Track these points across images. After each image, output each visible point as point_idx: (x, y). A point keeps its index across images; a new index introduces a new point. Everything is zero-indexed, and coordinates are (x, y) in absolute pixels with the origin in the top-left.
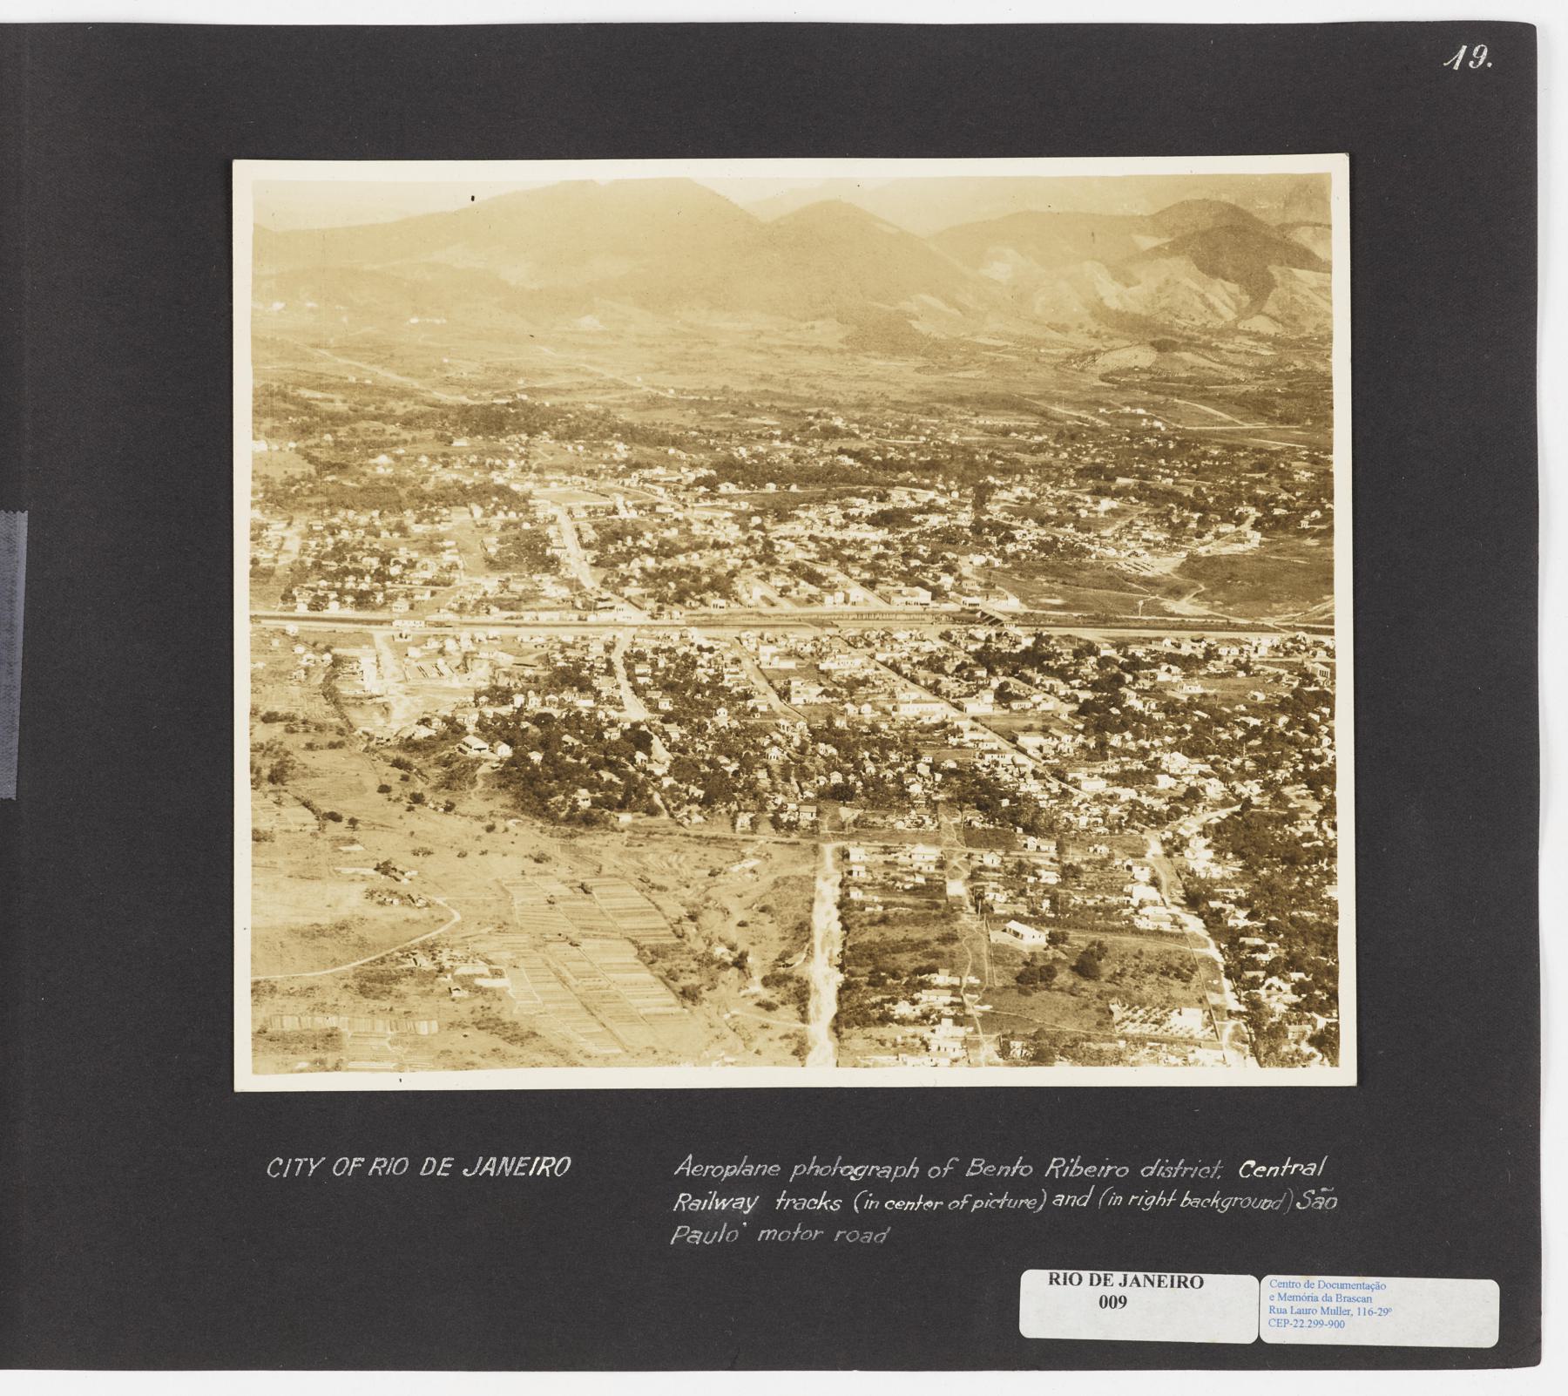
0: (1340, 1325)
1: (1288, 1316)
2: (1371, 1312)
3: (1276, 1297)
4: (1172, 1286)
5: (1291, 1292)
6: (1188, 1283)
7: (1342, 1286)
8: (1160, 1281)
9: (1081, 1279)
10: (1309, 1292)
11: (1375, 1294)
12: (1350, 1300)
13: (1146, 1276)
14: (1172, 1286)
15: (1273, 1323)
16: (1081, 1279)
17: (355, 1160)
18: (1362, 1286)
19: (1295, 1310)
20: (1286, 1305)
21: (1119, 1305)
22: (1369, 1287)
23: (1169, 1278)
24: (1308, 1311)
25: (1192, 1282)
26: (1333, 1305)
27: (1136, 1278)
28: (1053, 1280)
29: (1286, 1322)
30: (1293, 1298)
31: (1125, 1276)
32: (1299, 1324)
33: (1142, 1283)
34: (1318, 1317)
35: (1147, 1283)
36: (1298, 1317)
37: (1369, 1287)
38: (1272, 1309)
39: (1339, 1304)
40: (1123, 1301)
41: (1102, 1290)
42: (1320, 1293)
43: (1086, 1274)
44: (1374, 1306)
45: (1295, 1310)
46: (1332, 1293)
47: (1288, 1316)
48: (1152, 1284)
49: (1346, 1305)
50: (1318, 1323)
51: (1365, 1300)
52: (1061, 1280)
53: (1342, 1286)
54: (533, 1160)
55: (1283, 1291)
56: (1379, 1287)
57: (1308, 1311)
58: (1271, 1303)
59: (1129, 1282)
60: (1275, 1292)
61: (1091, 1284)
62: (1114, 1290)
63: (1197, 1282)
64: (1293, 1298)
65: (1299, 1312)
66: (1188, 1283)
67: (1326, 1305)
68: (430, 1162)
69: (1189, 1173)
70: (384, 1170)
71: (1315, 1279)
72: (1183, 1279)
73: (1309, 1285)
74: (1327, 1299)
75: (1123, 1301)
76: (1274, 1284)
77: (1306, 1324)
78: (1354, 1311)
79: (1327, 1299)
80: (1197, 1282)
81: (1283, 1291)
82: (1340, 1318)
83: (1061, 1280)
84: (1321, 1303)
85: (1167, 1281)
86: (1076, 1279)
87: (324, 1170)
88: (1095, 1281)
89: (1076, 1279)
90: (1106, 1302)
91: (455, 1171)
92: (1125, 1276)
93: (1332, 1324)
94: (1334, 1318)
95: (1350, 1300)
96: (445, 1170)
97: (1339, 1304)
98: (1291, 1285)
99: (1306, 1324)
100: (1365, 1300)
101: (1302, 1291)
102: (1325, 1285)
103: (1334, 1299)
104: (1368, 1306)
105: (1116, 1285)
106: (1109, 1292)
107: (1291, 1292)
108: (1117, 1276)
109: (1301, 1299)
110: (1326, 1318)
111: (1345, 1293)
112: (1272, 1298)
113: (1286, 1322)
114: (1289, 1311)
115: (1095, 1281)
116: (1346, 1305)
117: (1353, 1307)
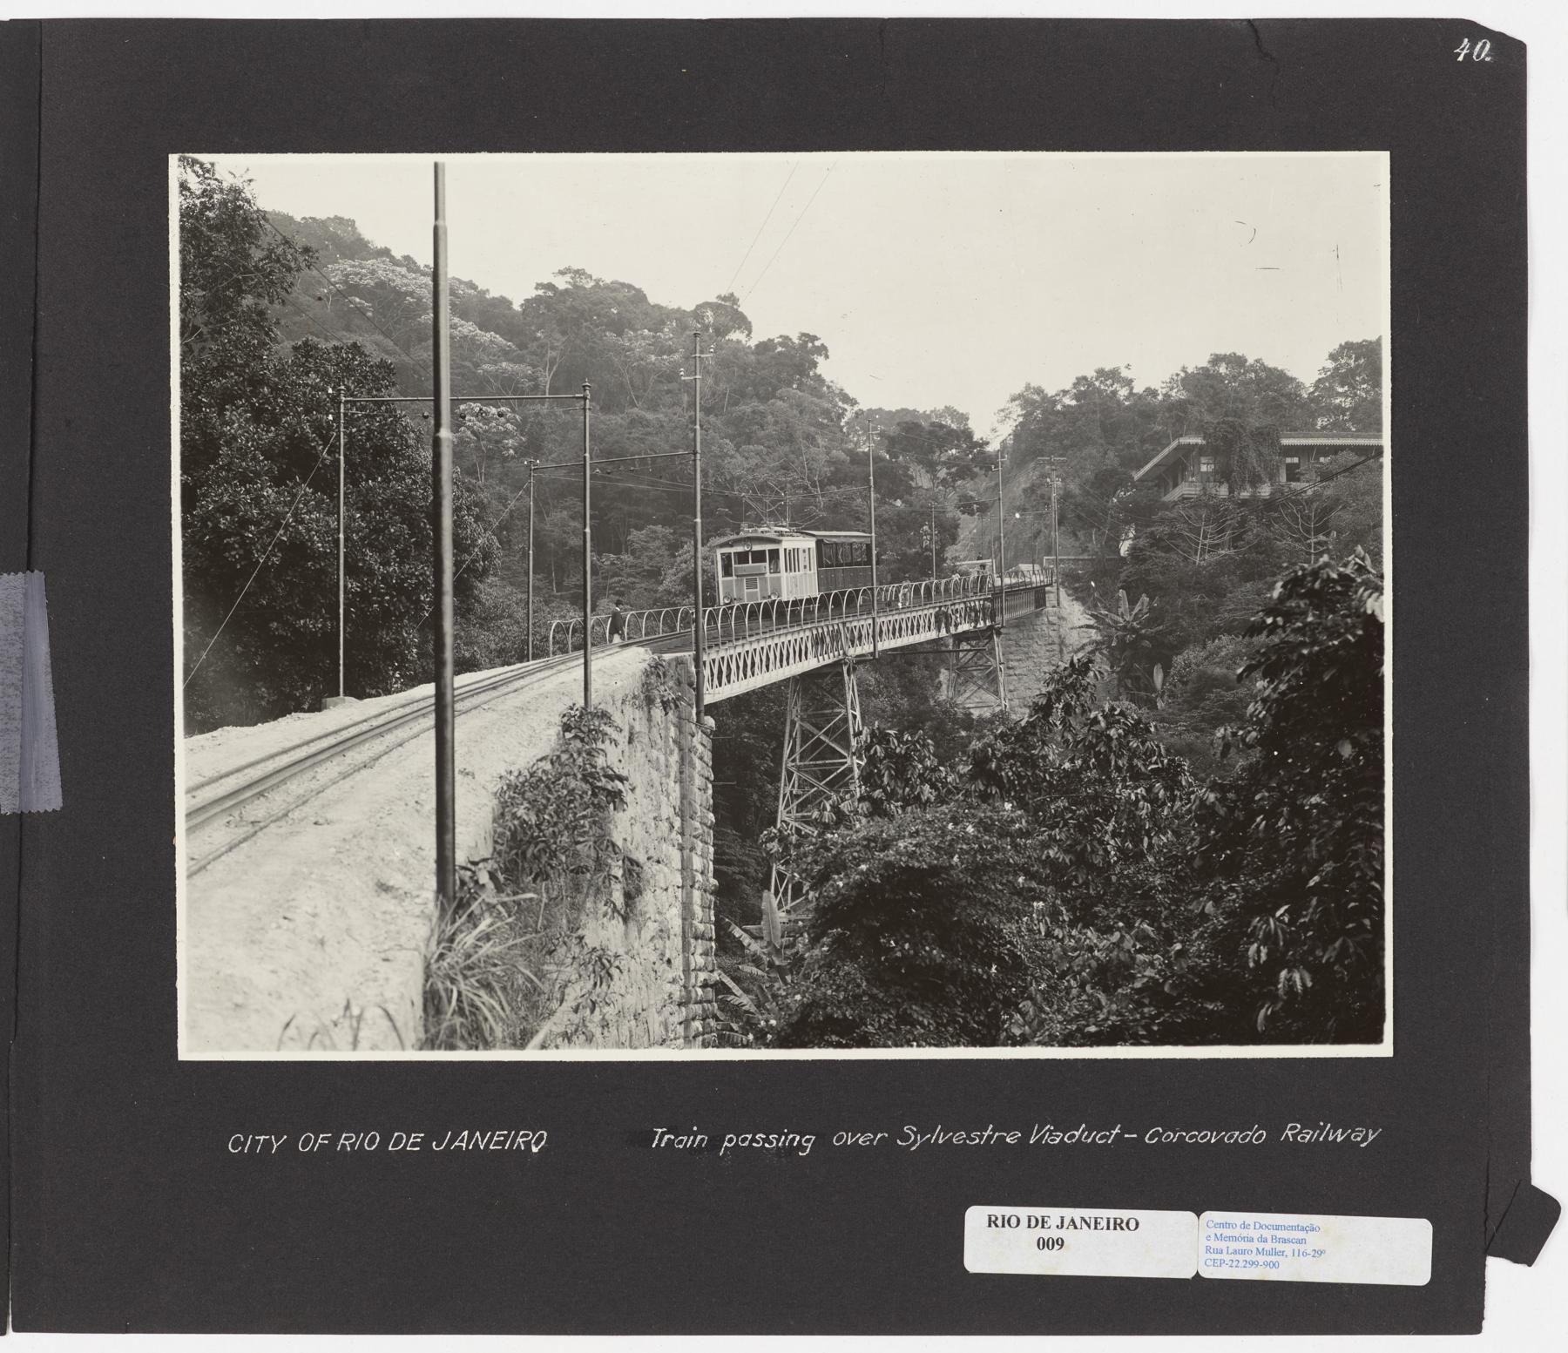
0: (1274, 1265)
1: (1226, 1258)
2: (1305, 1254)
3: (1213, 1237)
4: (1108, 1228)
5: (1228, 1232)
6: (1124, 1225)
7: (1277, 1228)
10: (1245, 1233)
11: (1310, 1236)
12: (1285, 1241)
13: (1083, 1219)
14: (1108, 1228)
15: (1209, 1262)
17: (321, 1136)
18: (1292, 1228)
20: (1222, 1245)
21: (1056, 1247)
22: (1303, 1229)
23: (1105, 1220)
24: (1243, 1252)
25: (1127, 1224)
26: (1268, 1246)
27: (1073, 1221)
28: (992, 1222)
29: (1222, 1262)
31: (1062, 1218)
33: (1079, 1227)
34: (1253, 1257)
36: (1232, 1257)
37: (1303, 1229)
38: (1208, 1249)
39: (1274, 1245)
41: (1039, 1232)
42: (1255, 1234)
43: (1023, 1212)
44: (1309, 1248)
46: (1266, 1233)
48: (1089, 1227)
49: (1280, 1247)
50: (1253, 1263)
51: (1301, 1241)
52: (999, 1222)
53: (1277, 1228)
55: (1219, 1231)
56: (1313, 1230)
57: (1243, 1252)
58: (1208, 1243)
59: (1066, 1225)
60: (1212, 1232)
61: (1029, 1226)
62: (1055, 1234)
65: (1235, 1252)
66: (1124, 1225)
67: (1261, 1246)
68: (400, 1138)
70: (352, 1145)
72: (1119, 1221)
73: (1245, 1226)
76: (1211, 1224)
78: (1288, 1252)
81: (1219, 1231)
82: (1273, 1258)
83: (999, 1222)
84: (1257, 1245)
85: (1104, 1223)
87: (289, 1147)
90: (1043, 1244)
91: (425, 1144)
92: (1062, 1218)
93: (1267, 1264)
94: (1269, 1259)
95: (1285, 1241)
96: (414, 1145)
97: (1274, 1245)
99: (1242, 1264)
100: (1301, 1241)
101: (1236, 1232)
102: (1261, 1227)
103: (1269, 1240)
104: (1302, 1247)
105: (1054, 1227)
106: (1045, 1234)
107: (1228, 1232)
108: (1054, 1214)
109: (1236, 1239)
110: (1261, 1259)
111: (1280, 1234)
112: (1208, 1238)
113: (1222, 1262)
114: (1225, 1252)
116: (1280, 1247)
117: (1288, 1248)
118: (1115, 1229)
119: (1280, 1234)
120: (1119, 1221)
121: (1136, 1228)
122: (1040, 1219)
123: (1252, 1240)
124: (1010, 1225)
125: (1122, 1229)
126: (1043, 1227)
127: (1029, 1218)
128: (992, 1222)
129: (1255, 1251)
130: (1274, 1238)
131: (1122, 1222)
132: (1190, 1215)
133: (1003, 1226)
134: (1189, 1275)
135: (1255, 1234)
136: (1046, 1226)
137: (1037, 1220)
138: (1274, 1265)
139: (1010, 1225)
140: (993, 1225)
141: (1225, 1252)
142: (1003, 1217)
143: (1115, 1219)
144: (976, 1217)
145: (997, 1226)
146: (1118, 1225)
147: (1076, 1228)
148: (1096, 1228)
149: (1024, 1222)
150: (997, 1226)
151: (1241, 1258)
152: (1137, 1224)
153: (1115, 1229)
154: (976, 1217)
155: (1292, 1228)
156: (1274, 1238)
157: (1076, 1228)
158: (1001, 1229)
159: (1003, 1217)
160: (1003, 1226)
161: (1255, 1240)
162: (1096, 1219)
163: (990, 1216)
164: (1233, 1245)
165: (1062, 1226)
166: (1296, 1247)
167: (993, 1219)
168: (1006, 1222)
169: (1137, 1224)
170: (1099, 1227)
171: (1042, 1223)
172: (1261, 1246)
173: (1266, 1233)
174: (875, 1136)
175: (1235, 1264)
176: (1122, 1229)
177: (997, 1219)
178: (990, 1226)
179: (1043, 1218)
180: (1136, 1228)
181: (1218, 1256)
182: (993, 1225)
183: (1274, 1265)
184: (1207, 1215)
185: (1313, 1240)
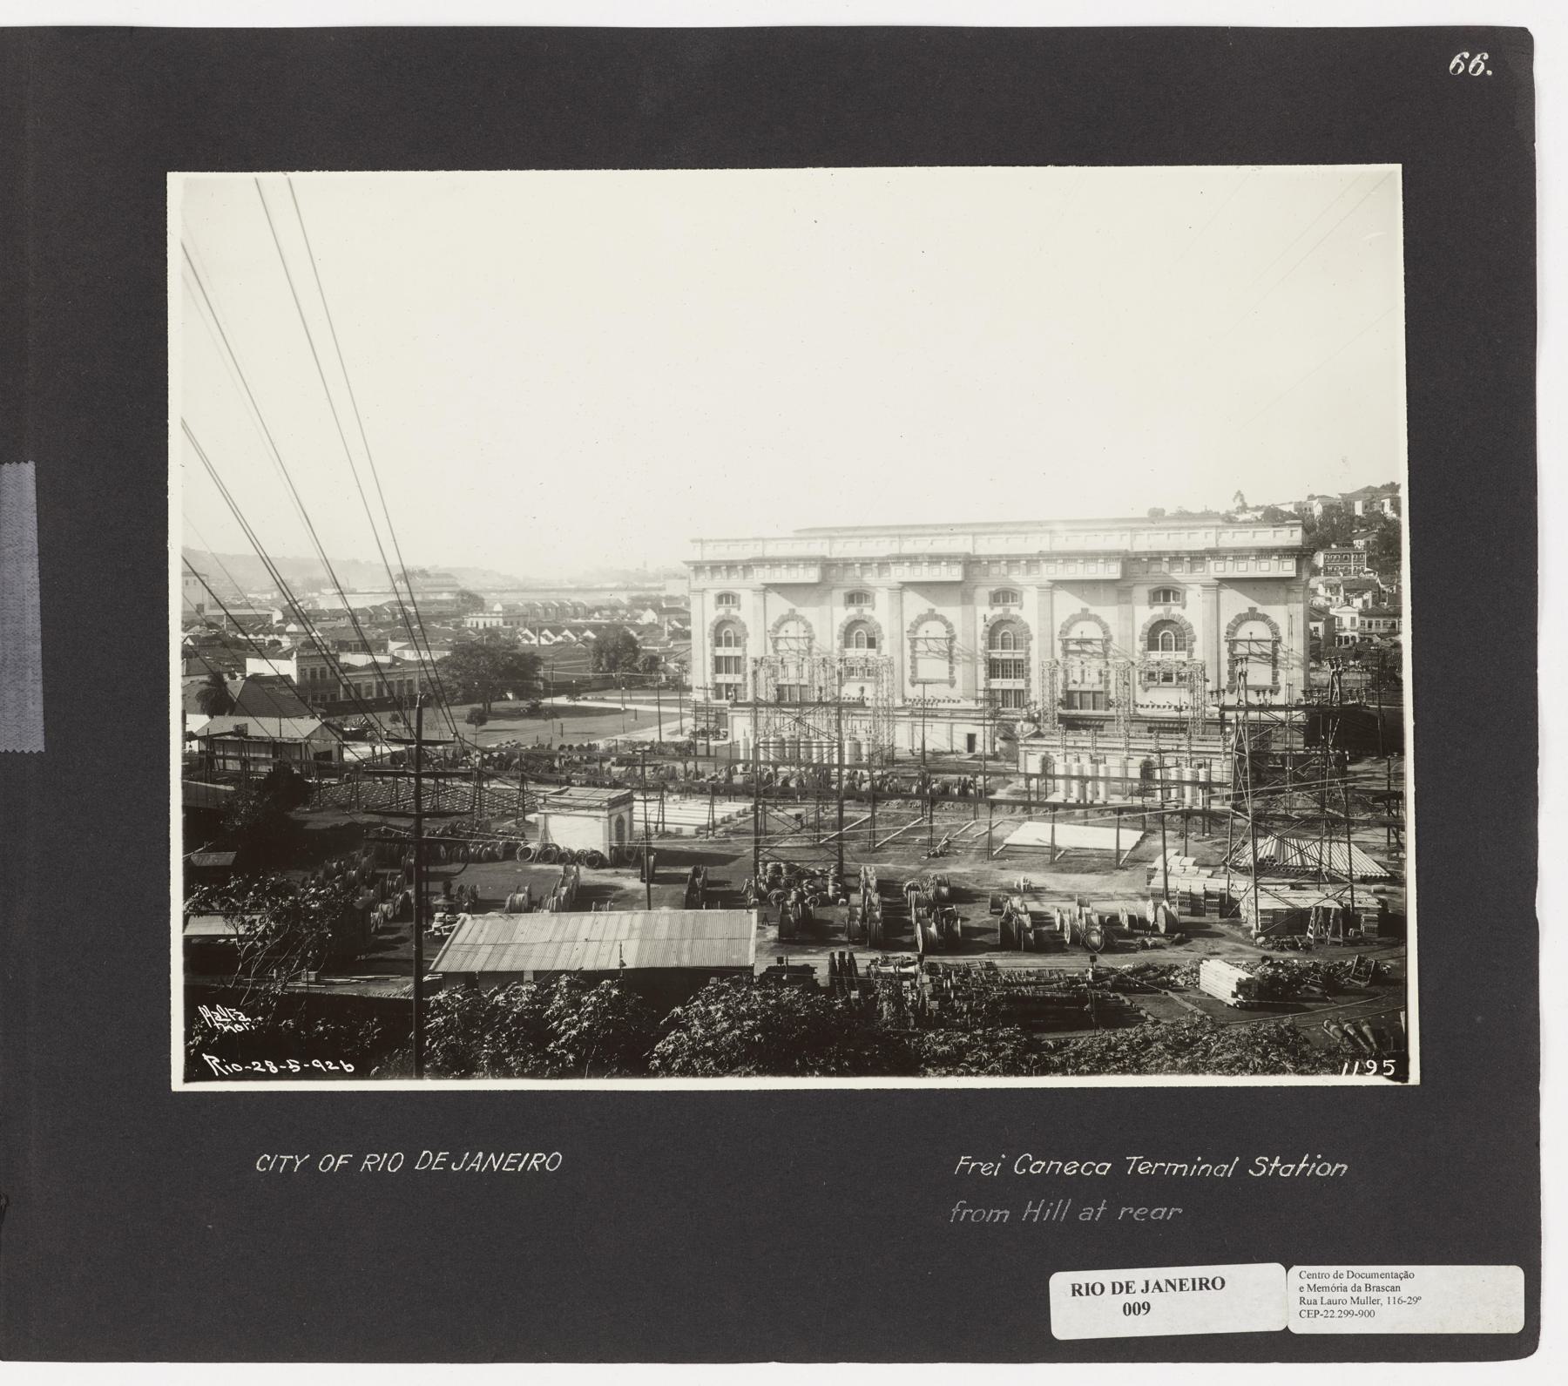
1: (1321, 1308)
2: (1400, 1301)
4: (1194, 1289)
5: (1320, 1282)
6: (1210, 1285)
7: (1370, 1276)
8: (1181, 1284)
9: (1103, 1289)
10: (1338, 1282)
11: (1404, 1283)
12: (1378, 1289)
13: (1168, 1281)
14: (1194, 1289)
16: (1103, 1289)
18: (1386, 1276)
19: (1325, 1301)
21: (1143, 1311)
22: (1397, 1276)
23: (1191, 1281)
26: (1363, 1295)
27: (1157, 1283)
28: (1076, 1291)
29: (1317, 1312)
30: (1326, 1288)
32: (1329, 1314)
33: (1164, 1289)
34: (1349, 1307)
35: (1169, 1286)
36: (1330, 1307)
37: (1397, 1276)
40: (1147, 1307)
42: (1349, 1283)
44: (1403, 1294)
45: (1325, 1301)
46: (1361, 1282)
47: (1321, 1308)
48: (1174, 1288)
49: (1374, 1295)
50: (1349, 1313)
51: (1393, 1289)
52: (1083, 1291)
53: (1370, 1276)
54: (522, 1157)
55: (1312, 1282)
56: (1407, 1276)
58: (1302, 1294)
61: (1114, 1292)
62: (1140, 1298)
63: (1218, 1283)
64: (1326, 1288)
65: (1330, 1302)
66: (1210, 1285)
67: (1355, 1295)
69: (1180, 1170)
71: (1343, 1269)
72: (1204, 1281)
73: (1338, 1276)
74: (1357, 1288)
75: (1147, 1307)
77: (1337, 1314)
78: (1384, 1301)
79: (1357, 1288)
80: (1218, 1283)
81: (1312, 1282)
83: (1083, 1291)
85: (1189, 1284)
86: (1098, 1289)
88: (1118, 1290)
89: (1098, 1289)
90: (1130, 1309)
95: (1378, 1289)
98: (1320, 1276)
99: (1337, 1314)
100: (1393, 1289)
101: (1329, 1282)
103: (1363, 1288)
104: (1396, 1294)
105: (1139, 1291)
110: (1356, 1308)
111: (1374, 1282)
113: (1317, 1312)
114: (1319, 1302)
115: (1118, 1290)
117: (1383, 1296)
118: (1201, 1289)
119: (1374, 1282)
120: (1204, 1281)
121: (1223, 1286)
122: (1124, 1285)
123: (1345, 1289)
124: (1094, 1293)
125: (1208, 1288)
126: (1128, 1292)
127: (1114, 1284)
128: (1076, 1291)
129: (1349, 1300)
130: (1368, 1287)
131: (1208, 1281)
132: (1277, 1268)
133: (1088, 1294)
134: (1280, 1328)
135: (1349, 1283)
136: (1130, 1291)
137: (1121, 1284)
138: (1369, 1314)
139: (1094, 1293)
140: (1077, 1293)
141: (1319, 1302)
142: (1087, 1285)
143: (1201, 1280)
144: (1060, 1283)
145: (1081, 1294)
146: (1204, 1284)
147: (1161, 1290)
148: (1181, 1289)
149: (1108, 1288)
150: (1081, 1294)
151: (1336, 1308)
152: (1223, 1282)
153: (1201, 1289)
154: (1060, 1283)
155: (1386, 1276)
156: (1368, 1287)
157: (1161, 1290)
158: (1085, 1298)
159: (1087, 1285)
160: (1088, 1294)
161: (1349, 1289)
162: (1181, 1281)
163: (1073, 1286)
164: (1327, 1296)
165: (1147, 1290)
166: (1392, 1294)
167: (1077, 1287)
168: (1090, 1289)
169: (1223, 1282)
170: (1184, 1288)
171: (1127, 1287)
172: (1355, 1295)
173: (1361, 1282)
174: (1153, 1165)
175: (1329, 1314)
176: (1208, 1288)
177: (1080, 1287)
178: (1074, 1295)
179: (1127, 1283)
180: (1223, 1286)
181: (1313, 1307)
182: (1077, 1293)
183: (1369, 1314)
184: (1296, 1269)
185: (1407, 1288)
